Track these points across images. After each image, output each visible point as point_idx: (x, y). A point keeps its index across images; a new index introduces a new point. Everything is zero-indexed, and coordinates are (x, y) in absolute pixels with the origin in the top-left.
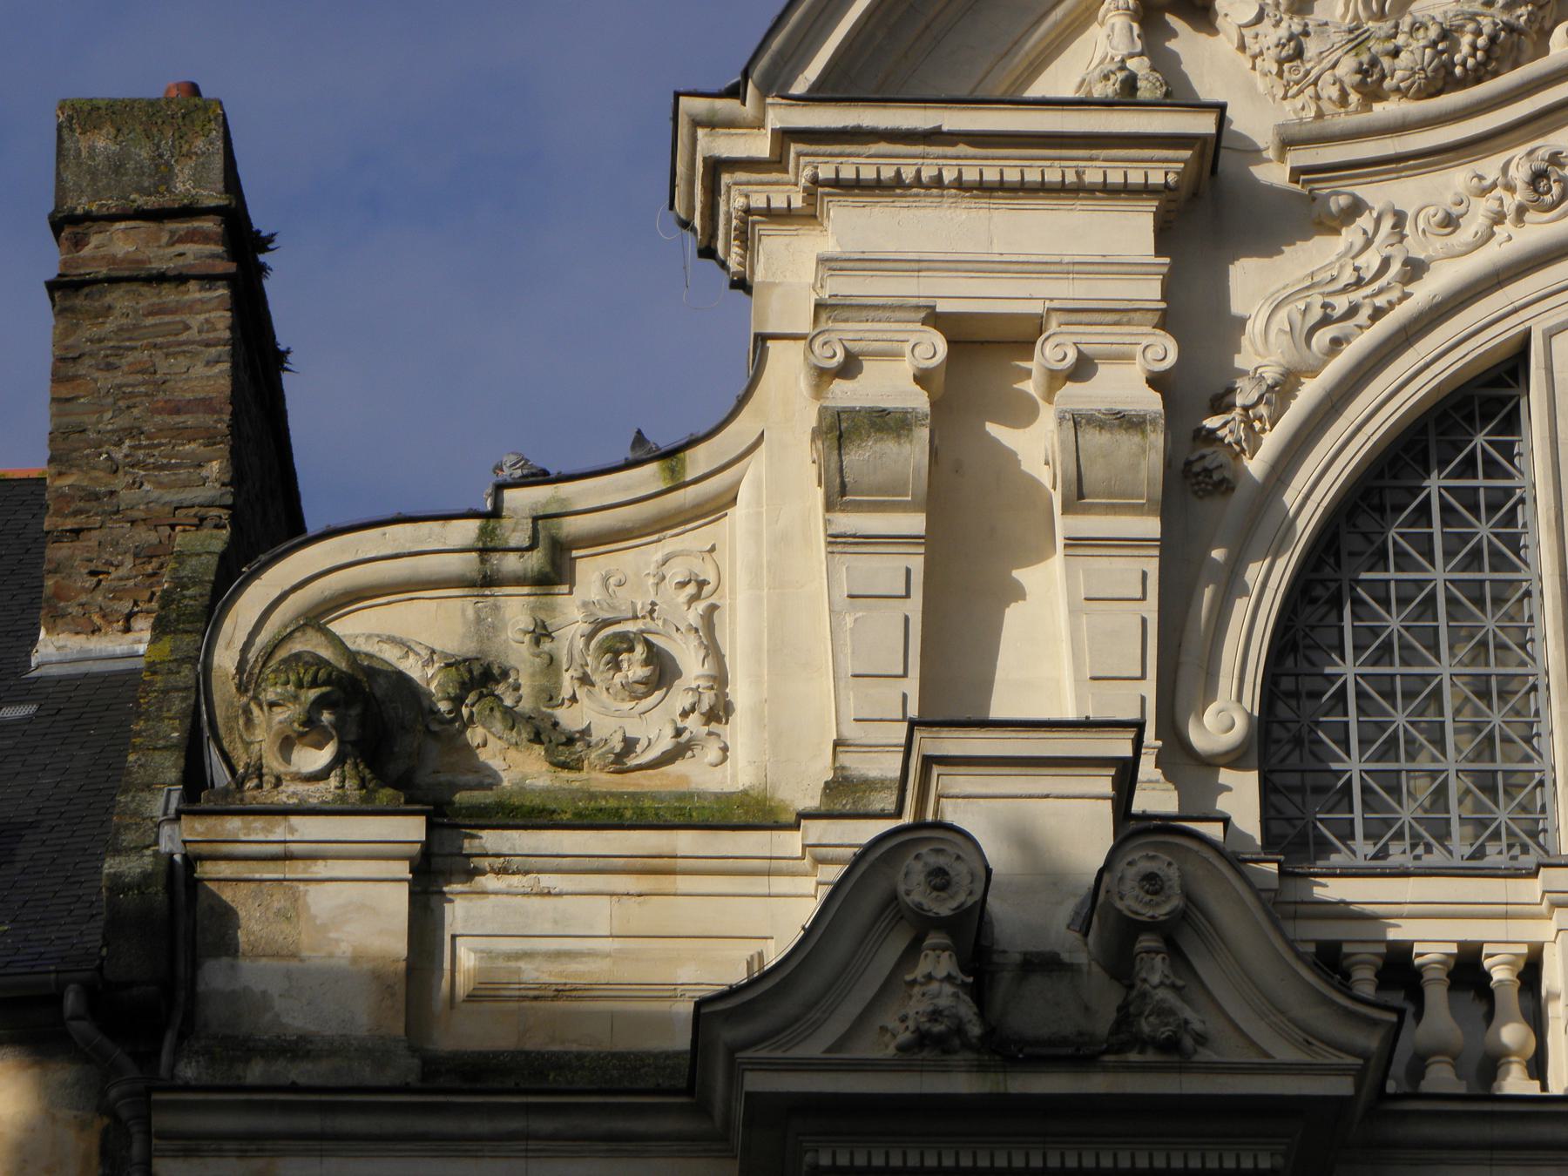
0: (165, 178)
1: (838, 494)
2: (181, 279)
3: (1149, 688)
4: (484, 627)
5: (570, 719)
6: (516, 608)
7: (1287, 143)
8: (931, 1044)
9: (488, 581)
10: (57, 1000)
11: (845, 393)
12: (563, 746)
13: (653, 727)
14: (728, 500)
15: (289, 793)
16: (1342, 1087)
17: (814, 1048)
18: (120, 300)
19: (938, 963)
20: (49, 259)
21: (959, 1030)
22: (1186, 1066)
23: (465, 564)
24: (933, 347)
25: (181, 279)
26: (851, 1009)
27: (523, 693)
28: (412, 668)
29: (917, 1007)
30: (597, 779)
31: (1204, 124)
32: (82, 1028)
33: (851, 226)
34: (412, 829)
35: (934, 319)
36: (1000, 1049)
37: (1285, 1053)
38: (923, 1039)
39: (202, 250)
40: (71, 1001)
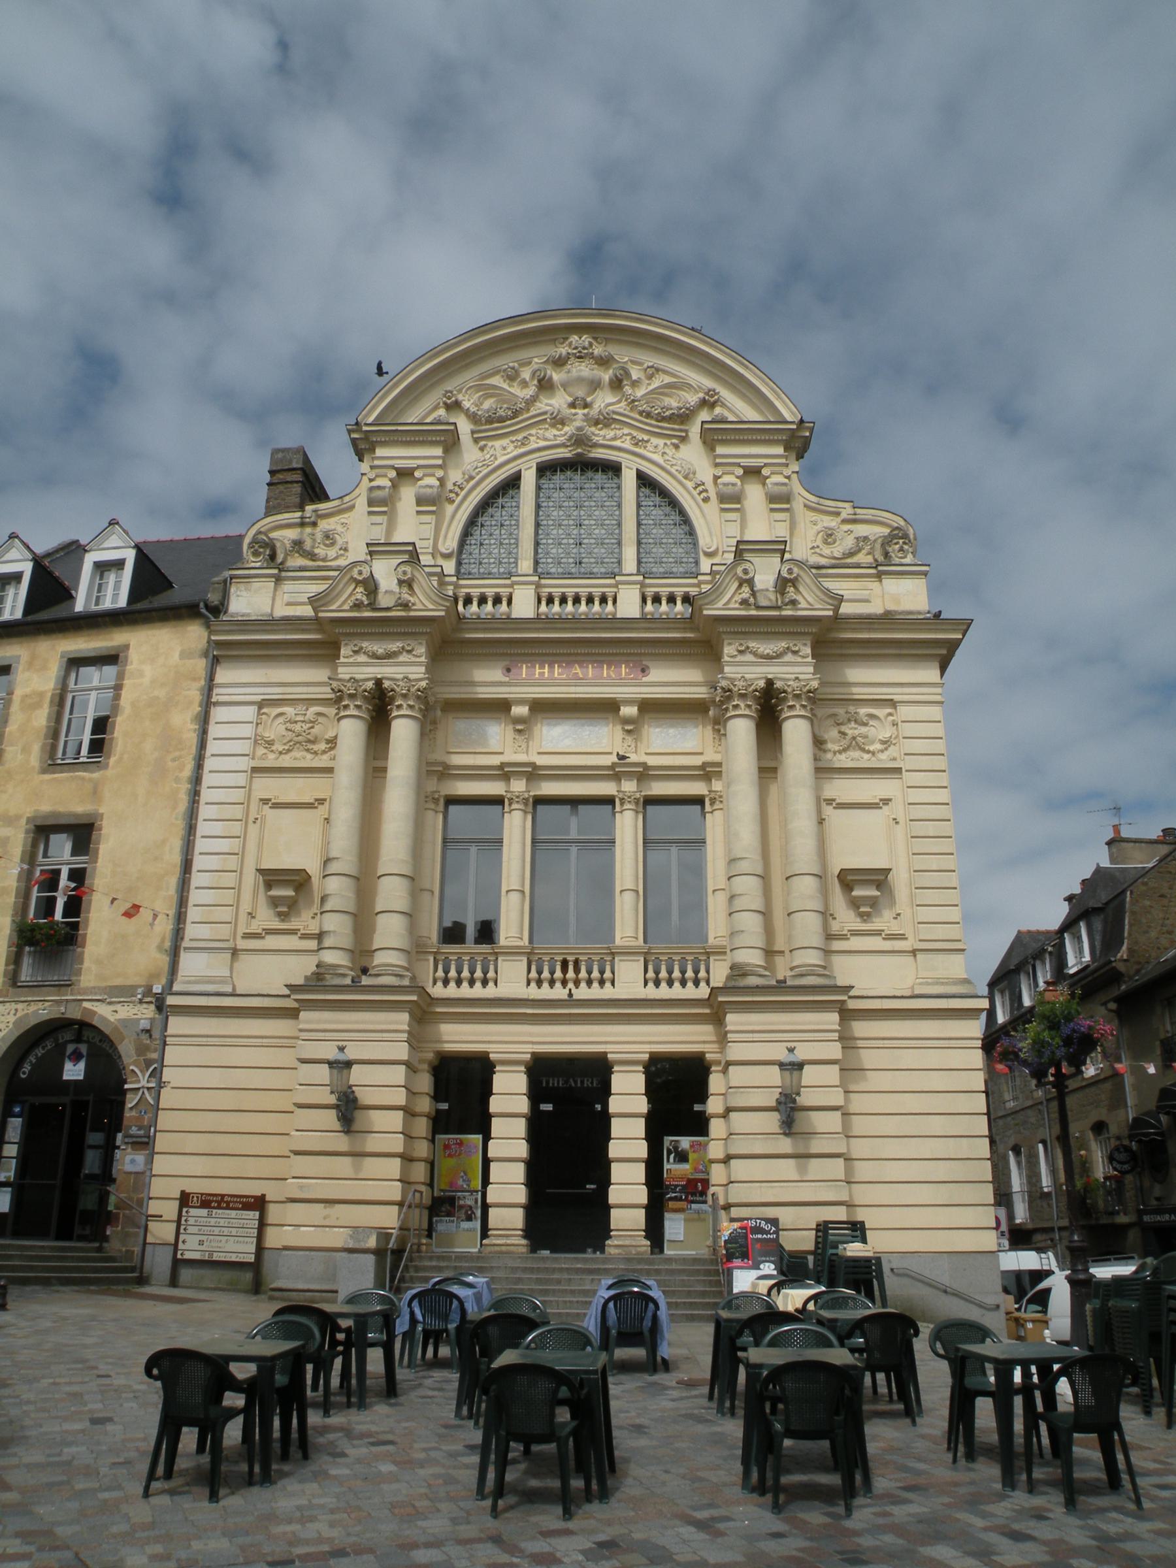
0: (291, 461)
1: (371, 503)
2: (291, 482)
3: (431, 541)
4: (302, 533)
5: (316, 551)
6: (308, 530)
7: (473, 432)
8: (357, 606)
9: (302, 524)
10: (197, 606)
11: (374, 484)
12: (312, 556)
13: (332, 553)
14: (353, 507)
15: (253, 565)
16: (443, 613)
17: (333, 607)
18: (281, 487)
19: (360, 589)
20: (268, 478)
21: (362, 602)
22: (410, 610)
23: (298, 520)
24: (393, 474)
25: (291, 482)
26: (342, 599)
27: (308, 545)
28: (286, 541)
29: (353, 598)
30: (321, 563)
31: (452, 427)
32: (204, 611)
33: (380, 452)
34: (275, 571)
35: (393, 467)
36: (372, 606)
37: (431, 607)
38: (355, 605)
39: (298, 477)
40: (202, 605)
